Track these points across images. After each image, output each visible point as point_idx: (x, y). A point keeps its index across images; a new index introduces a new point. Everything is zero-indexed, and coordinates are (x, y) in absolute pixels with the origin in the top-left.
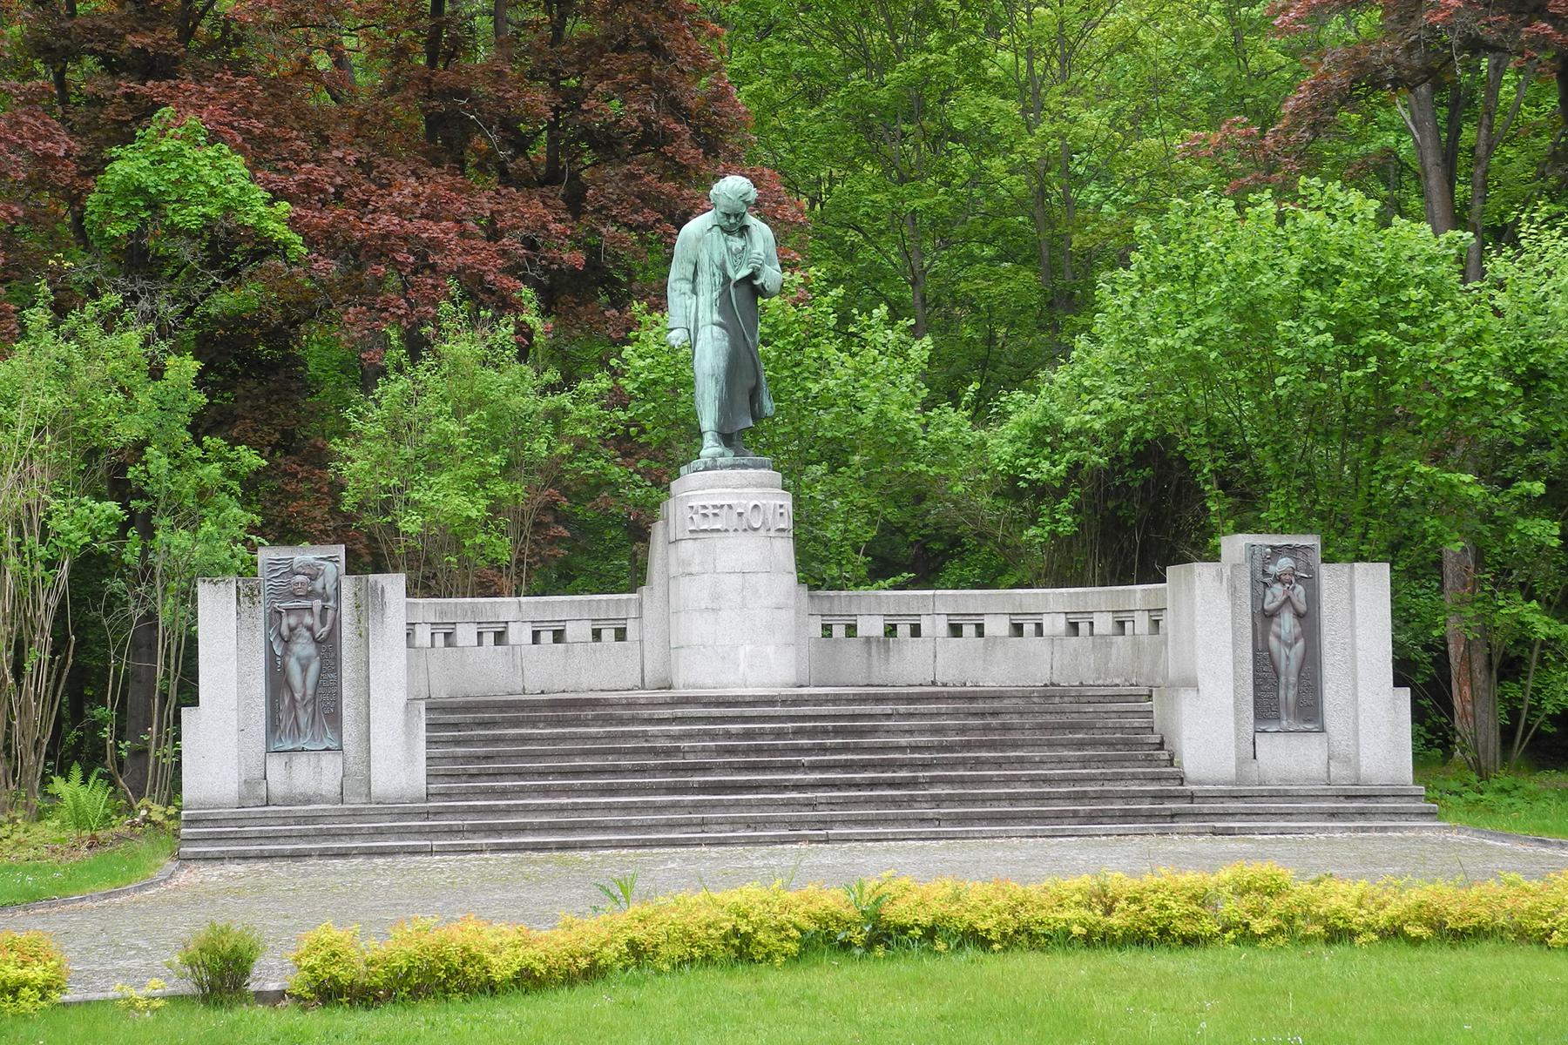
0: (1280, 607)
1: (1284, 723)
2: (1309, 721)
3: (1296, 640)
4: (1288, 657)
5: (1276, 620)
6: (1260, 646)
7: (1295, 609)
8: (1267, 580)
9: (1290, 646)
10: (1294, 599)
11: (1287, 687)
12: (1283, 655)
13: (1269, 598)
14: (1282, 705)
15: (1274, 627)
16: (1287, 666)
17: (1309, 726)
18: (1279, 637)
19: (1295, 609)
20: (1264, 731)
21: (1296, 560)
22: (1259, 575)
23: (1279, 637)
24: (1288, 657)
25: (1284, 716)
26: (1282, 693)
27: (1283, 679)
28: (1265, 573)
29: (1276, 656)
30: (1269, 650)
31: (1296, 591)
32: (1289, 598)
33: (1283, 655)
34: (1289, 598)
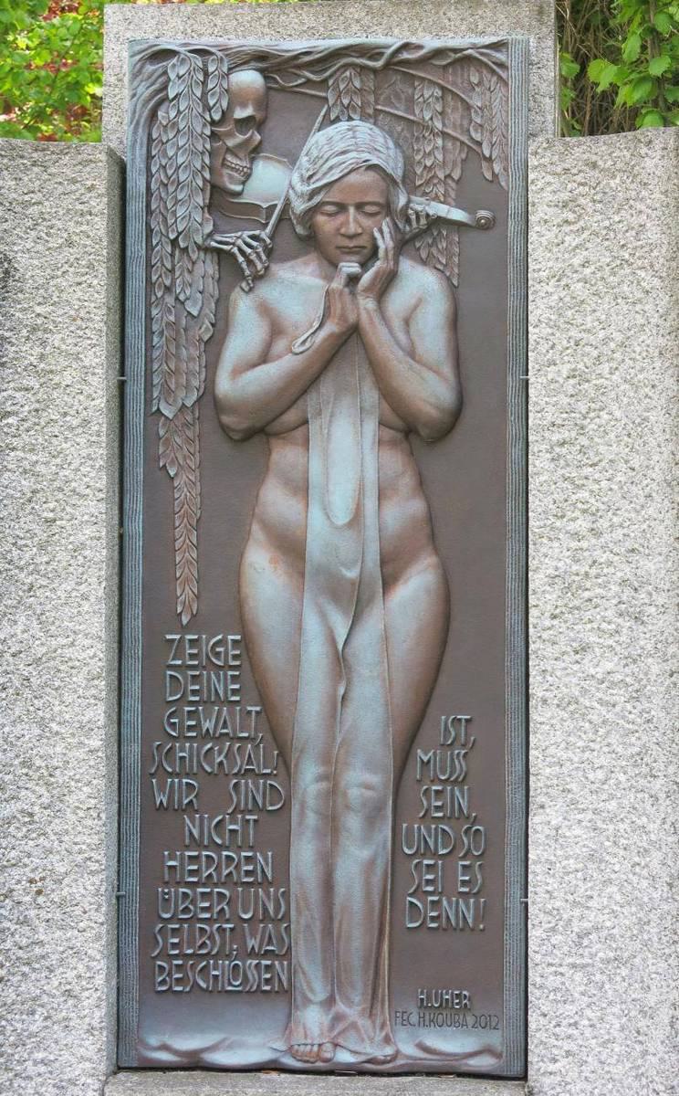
0: (306, 383)
1: (313, 1020)
2: (440, 1011)
3: (391, 570)
4: (341, 663)
5: (284, 455)
6: (185, 594)
7: (388, 394)
8: (237, 239)
9: (356, 601)
10: (382, 340)
11: (331, 827)
12: (315, 653)
13: (245, 335)
14: (306, 921)
15: (276, 499)
16: (337, 705)
17: (451, 1043)
18: (291, 548)
19: (388, 394)
20: (194, 1064)
21: (409, 131)
22: (189, 215)
23: (291, 548)
24: (341, 663)
25: (314, 982)
26: (304, 855)
27: (309, 778)
28: (220, 201)
29: (273, 654)
30: (238, 616)
31: (399, 300)
32: (350, 338)
33: (315, 653)
34: (350, 338)
